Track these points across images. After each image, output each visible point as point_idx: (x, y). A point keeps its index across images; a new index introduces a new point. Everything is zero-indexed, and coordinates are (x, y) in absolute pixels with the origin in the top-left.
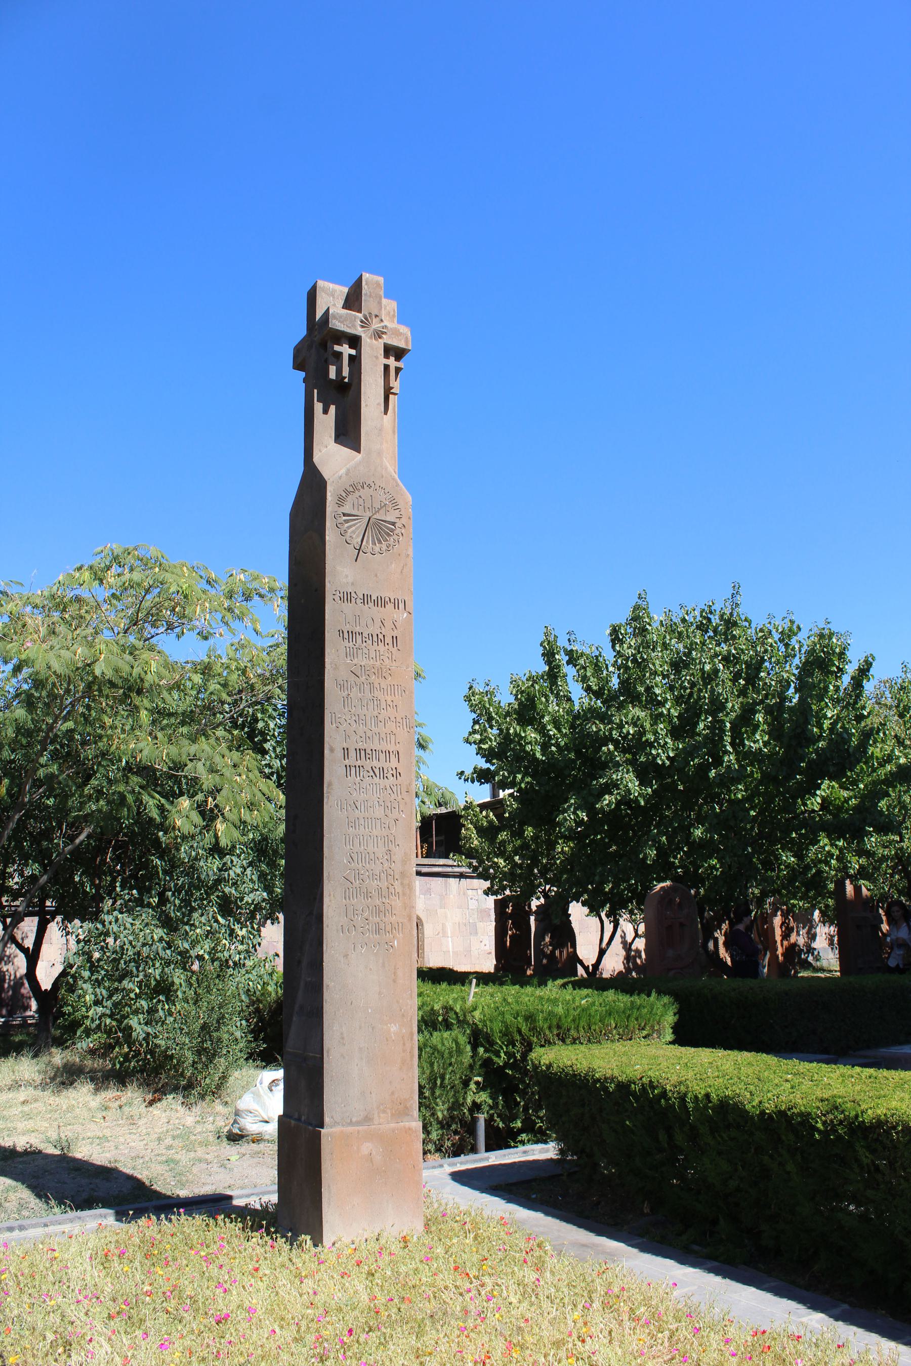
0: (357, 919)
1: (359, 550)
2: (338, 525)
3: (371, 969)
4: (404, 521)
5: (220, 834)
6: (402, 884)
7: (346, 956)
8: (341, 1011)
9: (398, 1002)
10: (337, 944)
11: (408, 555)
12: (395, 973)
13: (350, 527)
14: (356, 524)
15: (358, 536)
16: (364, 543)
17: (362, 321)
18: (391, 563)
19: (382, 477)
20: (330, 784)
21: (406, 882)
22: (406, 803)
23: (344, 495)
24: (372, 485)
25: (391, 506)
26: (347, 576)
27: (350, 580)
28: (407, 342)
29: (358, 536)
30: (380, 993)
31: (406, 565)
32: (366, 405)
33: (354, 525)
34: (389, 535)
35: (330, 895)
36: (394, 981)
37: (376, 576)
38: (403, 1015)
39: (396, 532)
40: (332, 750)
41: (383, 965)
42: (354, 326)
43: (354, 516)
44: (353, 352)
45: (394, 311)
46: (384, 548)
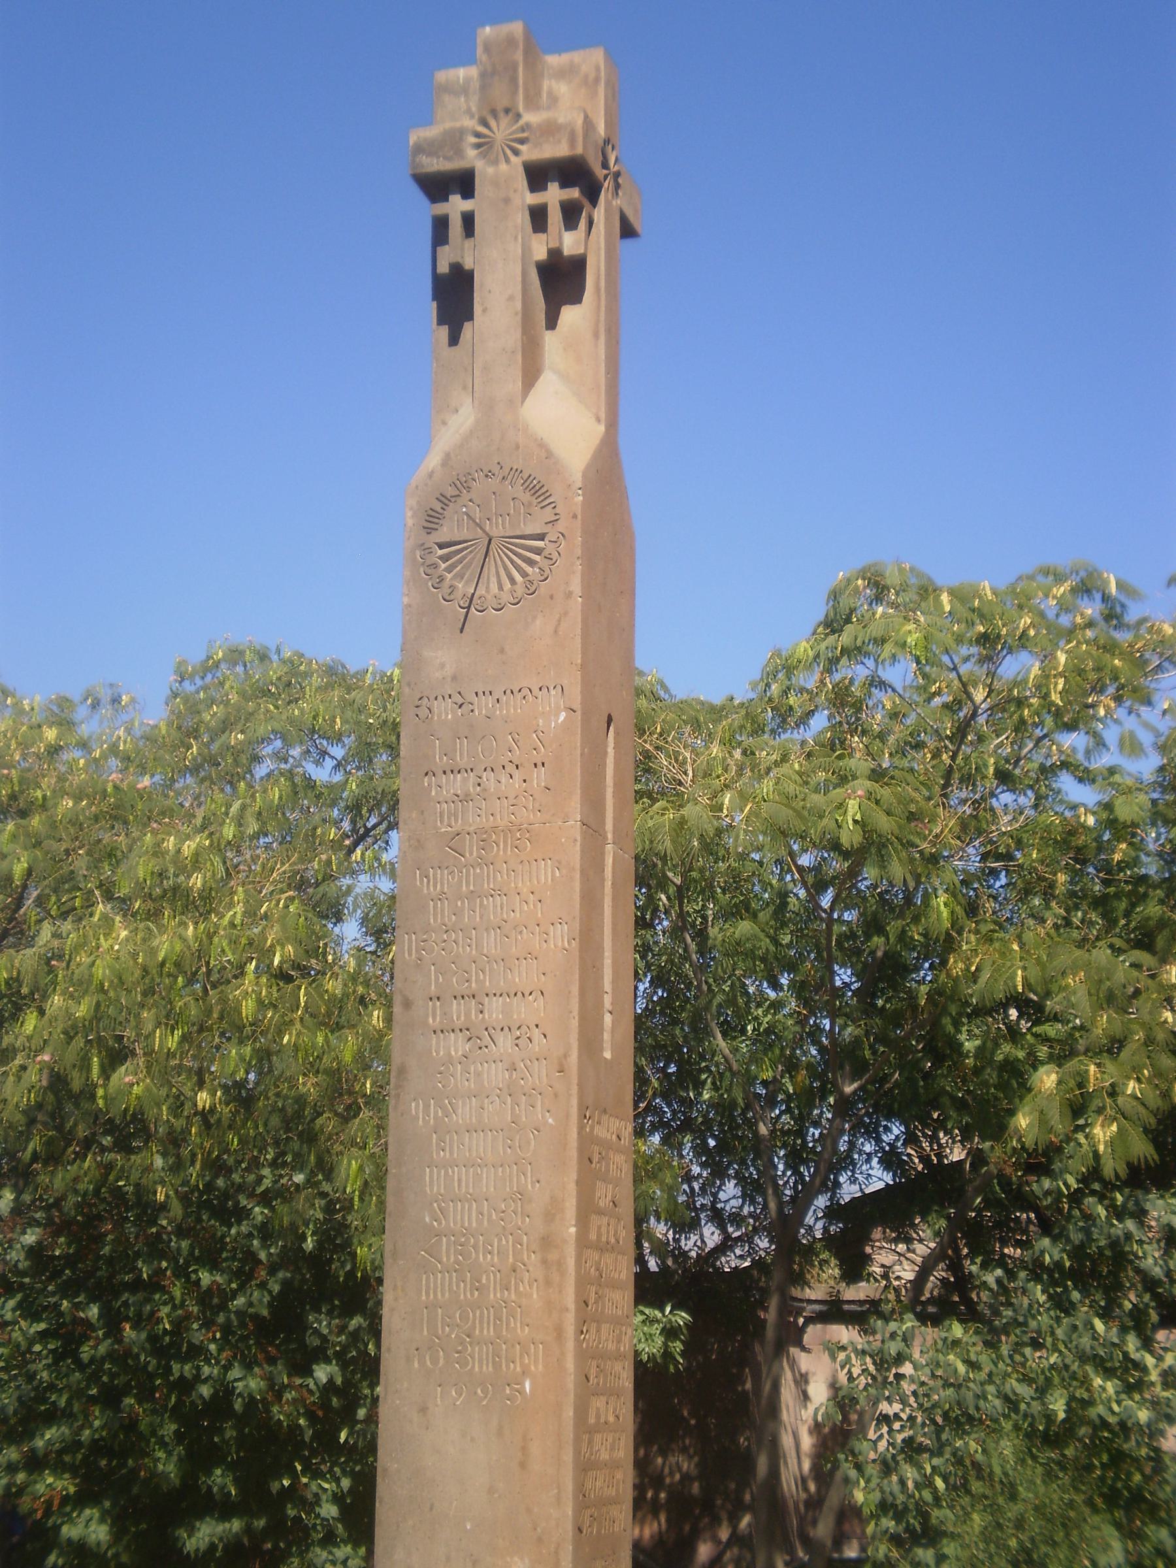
0: (449, 1336)
1: (469, 608)
2: (429, 571)
3: (472, 1439)
4: (561, 526)
5: (1101, 1148)
6: (544, 1262)
7: (423, 1410)
8: (410, 1523)
9: (529, 1511)
10: (406, 1385)
11: (571, 593)
12: (524, 1449)
13: (453, 566)
14: (464, 558)
15: (467, 583)
16: (481, 591)
17: (478, 135)
18: (534, 618)
19: (518, 447)
20: (402, 1071)
21: (553, 1256)
22: (556, 1095)
23: (438, 508)
24: (496, 470)
25: (535, 502)
26: (442, 666)
27: (449, 671)
28: (572, 142)
29: (467, 583)
30: (491, 1490)
31: (566, 614)
32: (485, 310)
33: (460, 561)
34: (531, 563)
35: (395, 1288)
36: (523, 1465)
37: (502, 651)
38: (540, 1540)
39: (545, 553)
40: (407, 1004)
41: (500, 1433)
42: (459, 153)
43: (460, 543)
44: (467, 205)
45: (598, 69)
46: (520, 590)
